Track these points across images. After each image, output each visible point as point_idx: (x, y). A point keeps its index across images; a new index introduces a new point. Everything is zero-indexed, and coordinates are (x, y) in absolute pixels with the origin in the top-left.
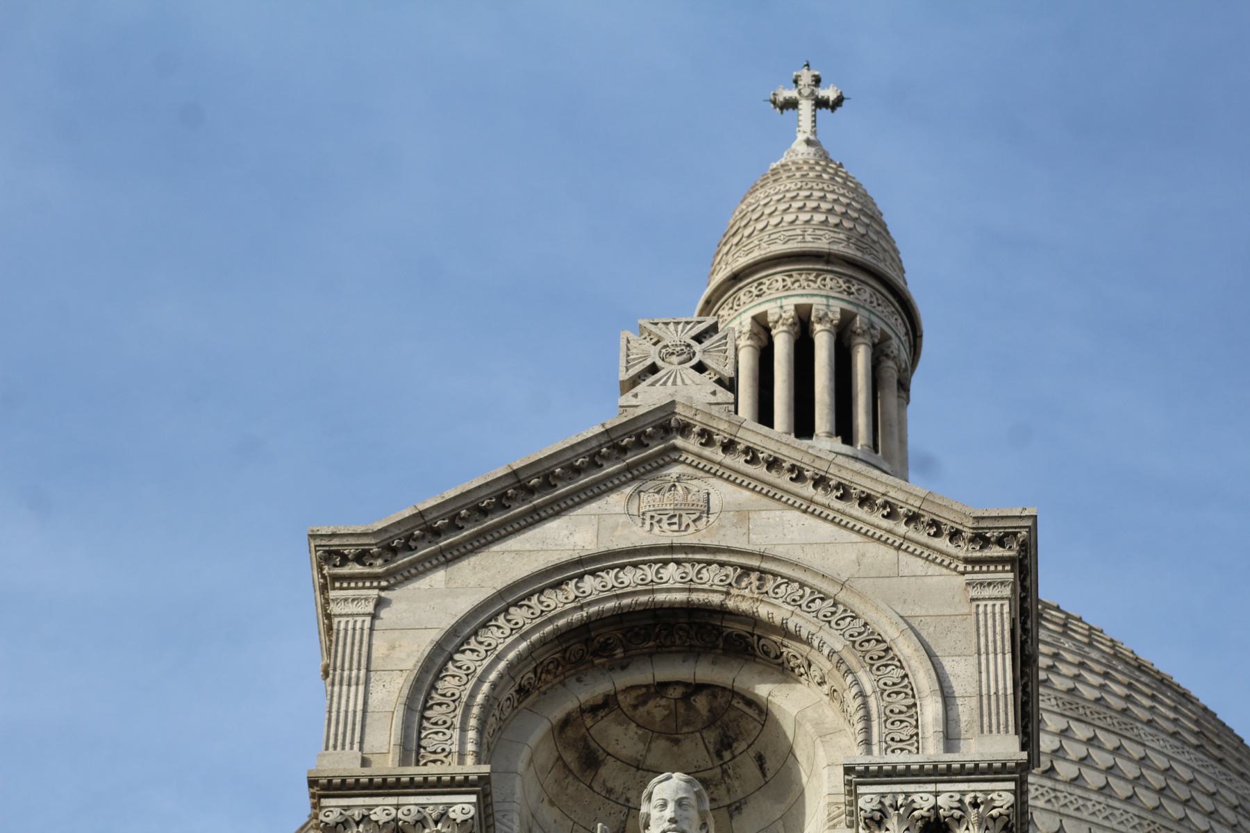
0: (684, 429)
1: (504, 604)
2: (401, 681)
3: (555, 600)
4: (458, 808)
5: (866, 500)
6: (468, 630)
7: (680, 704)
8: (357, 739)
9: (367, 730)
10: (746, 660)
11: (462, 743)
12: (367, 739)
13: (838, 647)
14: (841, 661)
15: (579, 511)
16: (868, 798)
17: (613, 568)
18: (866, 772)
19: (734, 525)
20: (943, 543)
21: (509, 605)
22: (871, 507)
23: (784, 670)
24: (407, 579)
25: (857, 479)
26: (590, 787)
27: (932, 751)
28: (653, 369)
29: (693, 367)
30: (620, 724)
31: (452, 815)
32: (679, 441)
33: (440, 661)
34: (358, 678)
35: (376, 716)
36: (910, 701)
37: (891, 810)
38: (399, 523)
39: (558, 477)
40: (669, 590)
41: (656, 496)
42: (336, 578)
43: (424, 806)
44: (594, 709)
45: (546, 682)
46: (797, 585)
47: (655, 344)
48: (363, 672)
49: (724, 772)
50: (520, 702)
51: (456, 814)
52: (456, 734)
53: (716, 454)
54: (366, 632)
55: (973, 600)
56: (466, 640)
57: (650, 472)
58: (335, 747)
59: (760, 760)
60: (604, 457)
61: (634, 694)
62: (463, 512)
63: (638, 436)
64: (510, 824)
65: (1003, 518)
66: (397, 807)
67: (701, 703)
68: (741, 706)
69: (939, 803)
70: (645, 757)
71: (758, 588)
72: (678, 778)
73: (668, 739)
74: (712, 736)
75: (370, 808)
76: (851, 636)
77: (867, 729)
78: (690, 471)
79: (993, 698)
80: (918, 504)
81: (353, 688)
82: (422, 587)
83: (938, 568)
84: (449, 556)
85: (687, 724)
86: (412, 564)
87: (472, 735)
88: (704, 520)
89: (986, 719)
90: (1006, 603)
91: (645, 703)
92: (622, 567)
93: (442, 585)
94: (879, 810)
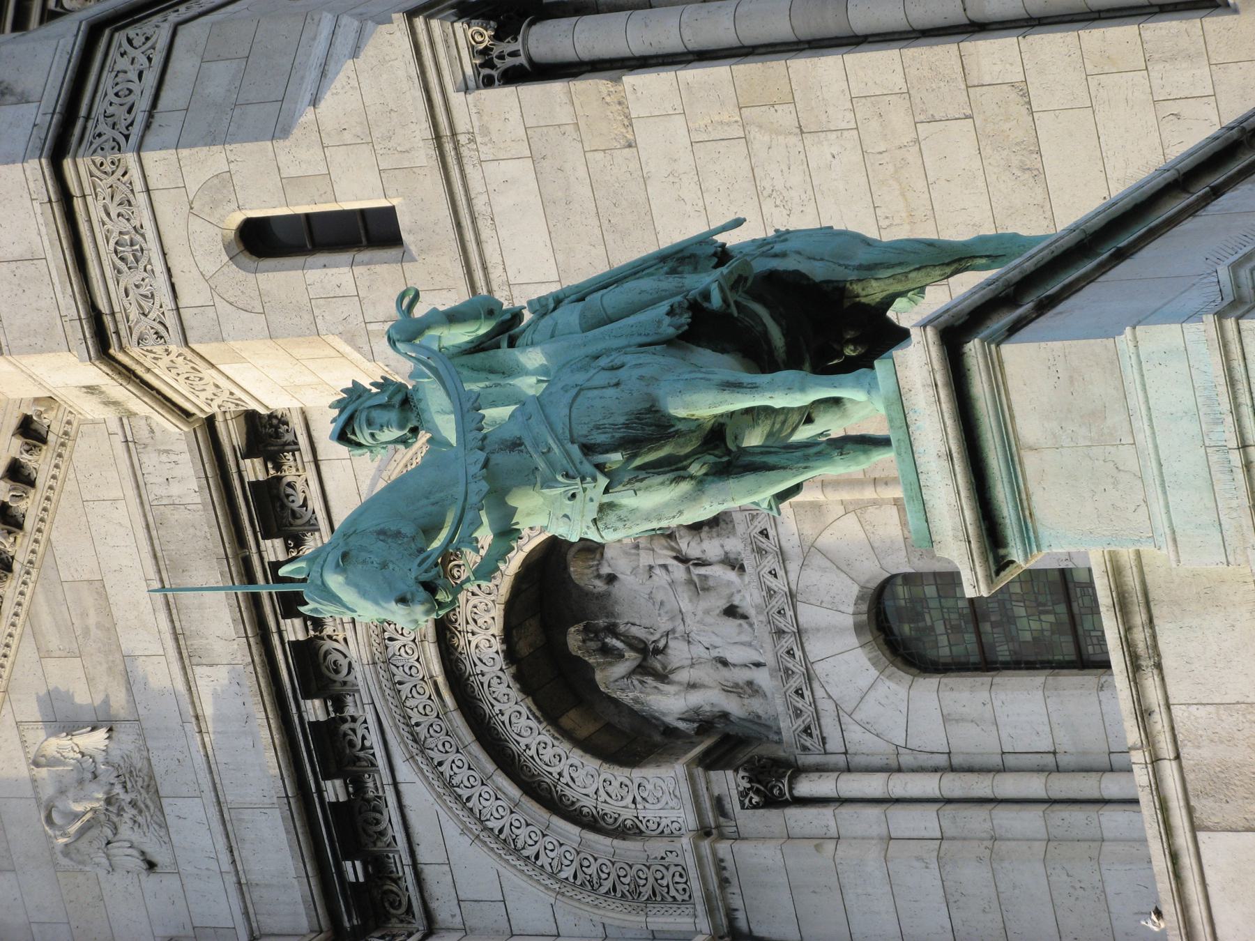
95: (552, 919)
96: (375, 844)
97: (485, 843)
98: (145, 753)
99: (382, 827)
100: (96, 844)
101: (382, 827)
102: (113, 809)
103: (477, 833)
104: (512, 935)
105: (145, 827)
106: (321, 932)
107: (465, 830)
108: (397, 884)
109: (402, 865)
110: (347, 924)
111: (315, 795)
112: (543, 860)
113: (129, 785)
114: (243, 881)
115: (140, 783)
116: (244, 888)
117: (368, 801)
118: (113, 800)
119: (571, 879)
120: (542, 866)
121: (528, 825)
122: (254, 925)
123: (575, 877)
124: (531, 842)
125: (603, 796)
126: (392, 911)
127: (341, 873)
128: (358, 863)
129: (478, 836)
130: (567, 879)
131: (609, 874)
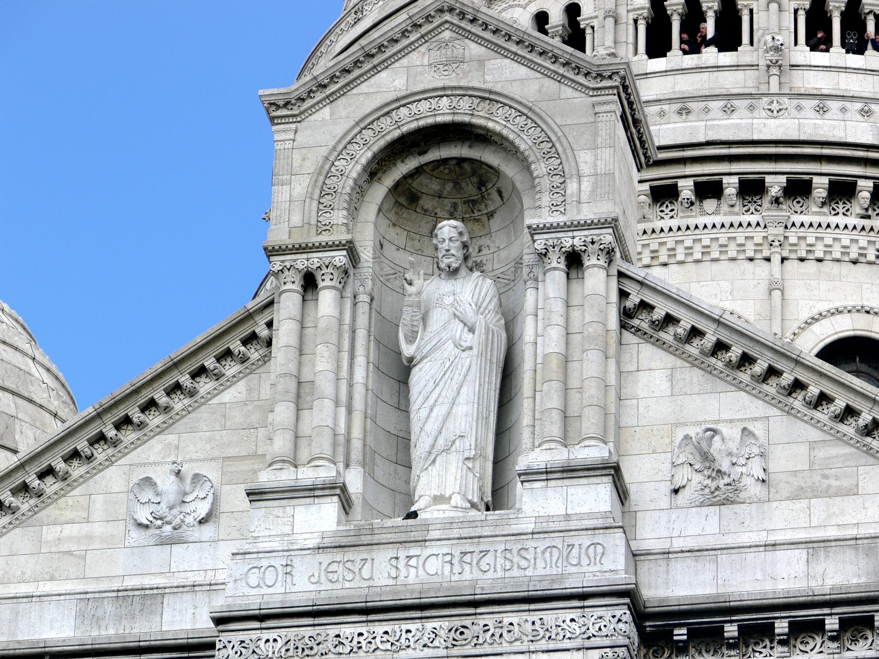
4: (337, 259)
6: (340, 147)
7: (456, 167)
10: (487, 144)
16: (539, 242)
17: (414, 102)
20: (580, 79)
24: (310, 115)
26: (416, 211)
33: (327, 167)
36: (562, 180)
40: (443, 114)
41: (438, 52)
45: (385, 165)
49: (483, 197)
50: (371, 179)
55: (595, 114)
56: (341, 153)
59: (500, 193)
61: (432, 165)
64: (368, 254)
67: (467, 166)
69: (575, 243)
73: (453, 182)
74: (475, 180)
76: (534, 139)
85: (461, 175)
86: (312, 106)
91: (438, 168)
92: (420, 100)
93: (328, 117)
94: (546, 249)
96: (693, 647)
98: (748, 501)
100: (690, 456)
105: (702, 493)
110: (647, 624)
111: (729, 618)
113: (729, 487)
114: (671, 556)
115: (731, 495)
116: (666, 556)
117: (720, 648)
118: (719, 474)
122: (642, 558)
126: (651, 651)
127: (680, 626)
128: (685, 637)
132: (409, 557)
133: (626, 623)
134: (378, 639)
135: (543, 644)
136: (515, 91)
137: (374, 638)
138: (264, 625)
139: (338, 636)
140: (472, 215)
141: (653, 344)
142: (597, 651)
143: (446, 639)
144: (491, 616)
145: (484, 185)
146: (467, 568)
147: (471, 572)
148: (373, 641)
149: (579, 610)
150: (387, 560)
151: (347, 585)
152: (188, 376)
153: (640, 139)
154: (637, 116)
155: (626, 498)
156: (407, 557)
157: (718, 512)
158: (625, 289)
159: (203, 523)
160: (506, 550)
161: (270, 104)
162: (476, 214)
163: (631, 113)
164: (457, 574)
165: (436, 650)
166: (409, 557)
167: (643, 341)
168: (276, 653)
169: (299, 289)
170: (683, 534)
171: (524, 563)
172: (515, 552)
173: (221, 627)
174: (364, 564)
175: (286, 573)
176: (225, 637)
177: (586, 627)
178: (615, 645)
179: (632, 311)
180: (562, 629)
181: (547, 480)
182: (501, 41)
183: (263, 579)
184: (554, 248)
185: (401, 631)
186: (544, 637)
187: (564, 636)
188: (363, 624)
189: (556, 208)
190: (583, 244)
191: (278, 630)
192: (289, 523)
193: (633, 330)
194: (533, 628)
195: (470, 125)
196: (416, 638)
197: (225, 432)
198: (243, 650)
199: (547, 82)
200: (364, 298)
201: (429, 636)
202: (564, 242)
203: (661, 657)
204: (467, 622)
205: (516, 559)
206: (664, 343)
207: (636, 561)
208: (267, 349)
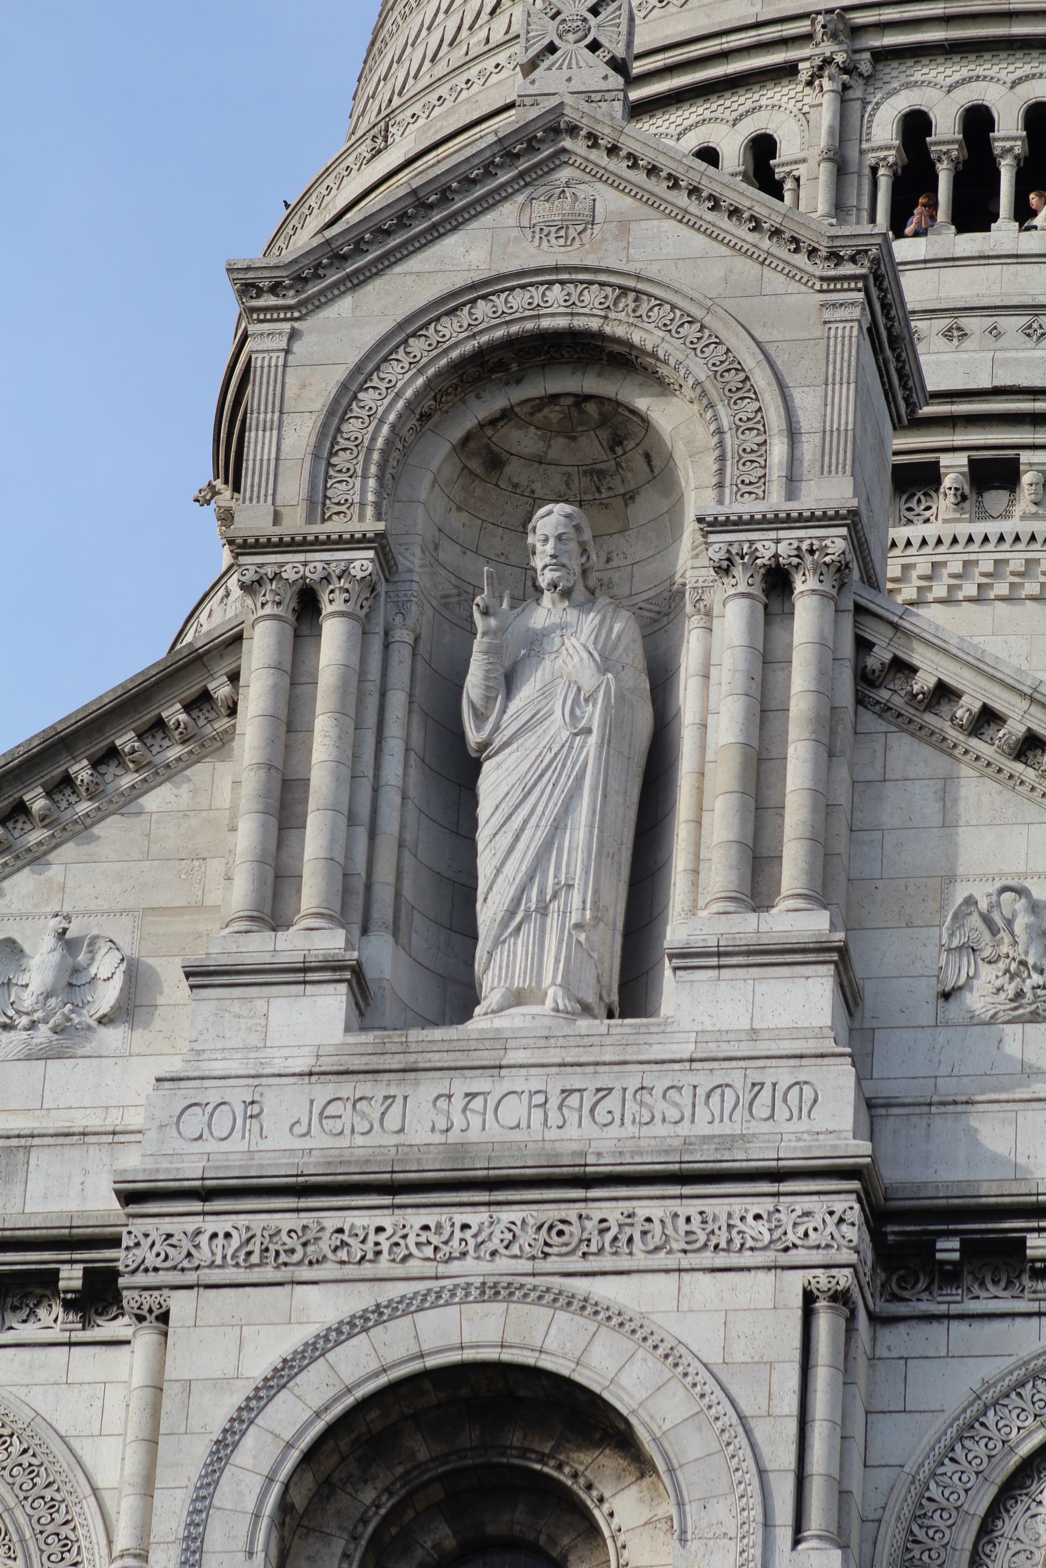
0: (573, 130)
1: (404, 335)
2: (310, 424)
3: (450, 329)
4: (357, 564)
5: (734, 212)
6: (370, 366)
8: (270, 492)
9: (280, 480)
11: (363, 491)
12: (279, 489)
13: (702, 377)
14: (704, 393)
15: (475, 224)
16: (716, 547)
17: (503, 291)
18: (715, 522)
19: (616, 238)
20: (801, 260)
21: (409, 336)
22: (739, 219)
23: (662, 386)
24: (318, 307)
25: (726, 192)
26: (497, 485)
27: (775, 501)
28: (552, 48)
29: (588, 47)
30: (520, 428)
31: (353, 572)
32: (567, 143)
33: (345, 401)
34: (272, 421)
35: (288, 464)
36: (760, 439)
37: (737, 559)
38: (308, 252)
39: (456, 191)
40: (553, 315)
42: (253, 310)
43: (328, 563)
44: (493, 422)
45: (448, 402)
46: (668, 307)
47: (553, 18)
48: (277, 415)
49: (618, 464)
51: (356, 571)
52: (358, 482)
53: (599, 157)
54: (280, 369)
55: (825, 322)
56: (369, 378)
57: (541, 176)
58: (251, 500)
59: (648, 457)
60: (497, 166)
61: (530, 405)
62: (367, 236)
63: (529, 142)
64: (411, 558)
65: (855, 236)
66: (305, 564)
67: (591, 408)
68: (626, 413)
70: (546, 453)
71: (634, 311)
72: (561, 509)
74: (604, 434)
75: (281, 565)
76: (714, 365)
77: (721, 471)
78: (578, 174)
79: (835, 434)
80: (779, 220)
81: (268, 433)
82: (332, 316)
83: (797, 284)
84: (355, 281)
86: (321, 292)
87: (372, 483)
88: (589, 231)
89: (827, 458)
90: (856, 324)
91: (540, 410)
92: (512, 289)
94: (728, 559)
95: (883, 1463)
96: (972, 1273)
97: (971, 1404)
99: (990, 1286)
101: (990, 1286)
102: (1013, 966)
103: (983, 1398)
104: (867, 1413)
106: (886, 1199)
107: (988, 1386)
108: (925, 1290)
109: (949, 1303)
112: (949, 1467)
117: (1019, 1277)
119: (927, 1495)
120: (943, 1464)
121: (990, 1457)
123: (930, 1499)
124: (970, 1457)
125: (1015, 1547)
126: (895, 1278)
128: (956, 1256)
129: (979, 1397)
130: (928, 1489)
131: (933, 1539)
132: (471, 1096)
133: (853, 1224)
134: (411, 1240)
135: (708, 1259)
136: (680, 277)
137: (405, 1237)
138: (209, 1207)
139: (340, 1231)
140: (597, 496)
141: (913, 735)
142: (801, 1272)
143: (532, 1243)
144: (614, 1204)
145: (620, 443)
146: (572, 1118)
147: (580, 1126)
148: (401, 1242)
149: (770, 1199)
150: (431, 1099)
151: (359, 1140)
152: (85, 762)
153: (900, 371)
154: (897, 329)
155: (856, 1005)
156: (467, 1095)
157: (1019, 1035)
158: (867, 636)
159: (105, 1025)
160: (643, 1088)
161: (247, 285)
162: (604, 495)
163: (885, 325)
164: (554, 1127)
165: (514, 1261)
166: (471, 1096)
167: (894, 729)
168: (229, 1257)
169: (290, 616)
170: (956, 1072)
171: (673, 1114)
172: (658, 1092)
173: (134, 1209)
174: (390, 1105)
175: (251, 1117)
176: (138, 1227)
177: (780, 1231)
178: (832, 1262)
179: (877, 673)
180: (739, 1232)
181: (719, 967)
182: (659, 187)
183: (209, 1125)
184: (742, 558)
185: (453, 1225)
186: (706, 1245)
187: (742, 1245)
188: (385, 1212)
189: (749, 489)
190: (795, 553)
191: (233, 1217)
192: (259, 1028)
193: (878, 707)
194: (688, 1228)
195: (600, 335)
196: (480, 1239)
197: (147, 863)
198: (171, 1251)
199: (742, 263)
200: (403, 635)
201: (502, 1236)
202: (760, 548)
203: (912, 1288)
204: (571, 1212)
205: (660, 1106)
206: (933, 733)
207: (872, 1118)
208: (227, 720)
